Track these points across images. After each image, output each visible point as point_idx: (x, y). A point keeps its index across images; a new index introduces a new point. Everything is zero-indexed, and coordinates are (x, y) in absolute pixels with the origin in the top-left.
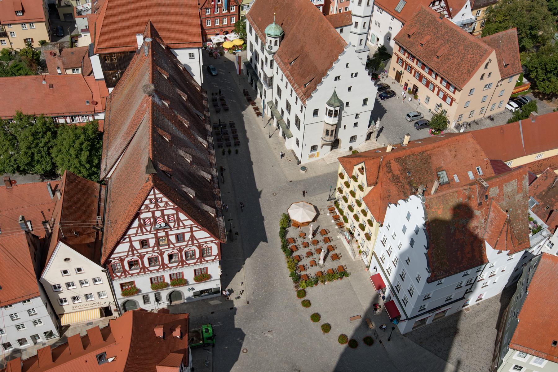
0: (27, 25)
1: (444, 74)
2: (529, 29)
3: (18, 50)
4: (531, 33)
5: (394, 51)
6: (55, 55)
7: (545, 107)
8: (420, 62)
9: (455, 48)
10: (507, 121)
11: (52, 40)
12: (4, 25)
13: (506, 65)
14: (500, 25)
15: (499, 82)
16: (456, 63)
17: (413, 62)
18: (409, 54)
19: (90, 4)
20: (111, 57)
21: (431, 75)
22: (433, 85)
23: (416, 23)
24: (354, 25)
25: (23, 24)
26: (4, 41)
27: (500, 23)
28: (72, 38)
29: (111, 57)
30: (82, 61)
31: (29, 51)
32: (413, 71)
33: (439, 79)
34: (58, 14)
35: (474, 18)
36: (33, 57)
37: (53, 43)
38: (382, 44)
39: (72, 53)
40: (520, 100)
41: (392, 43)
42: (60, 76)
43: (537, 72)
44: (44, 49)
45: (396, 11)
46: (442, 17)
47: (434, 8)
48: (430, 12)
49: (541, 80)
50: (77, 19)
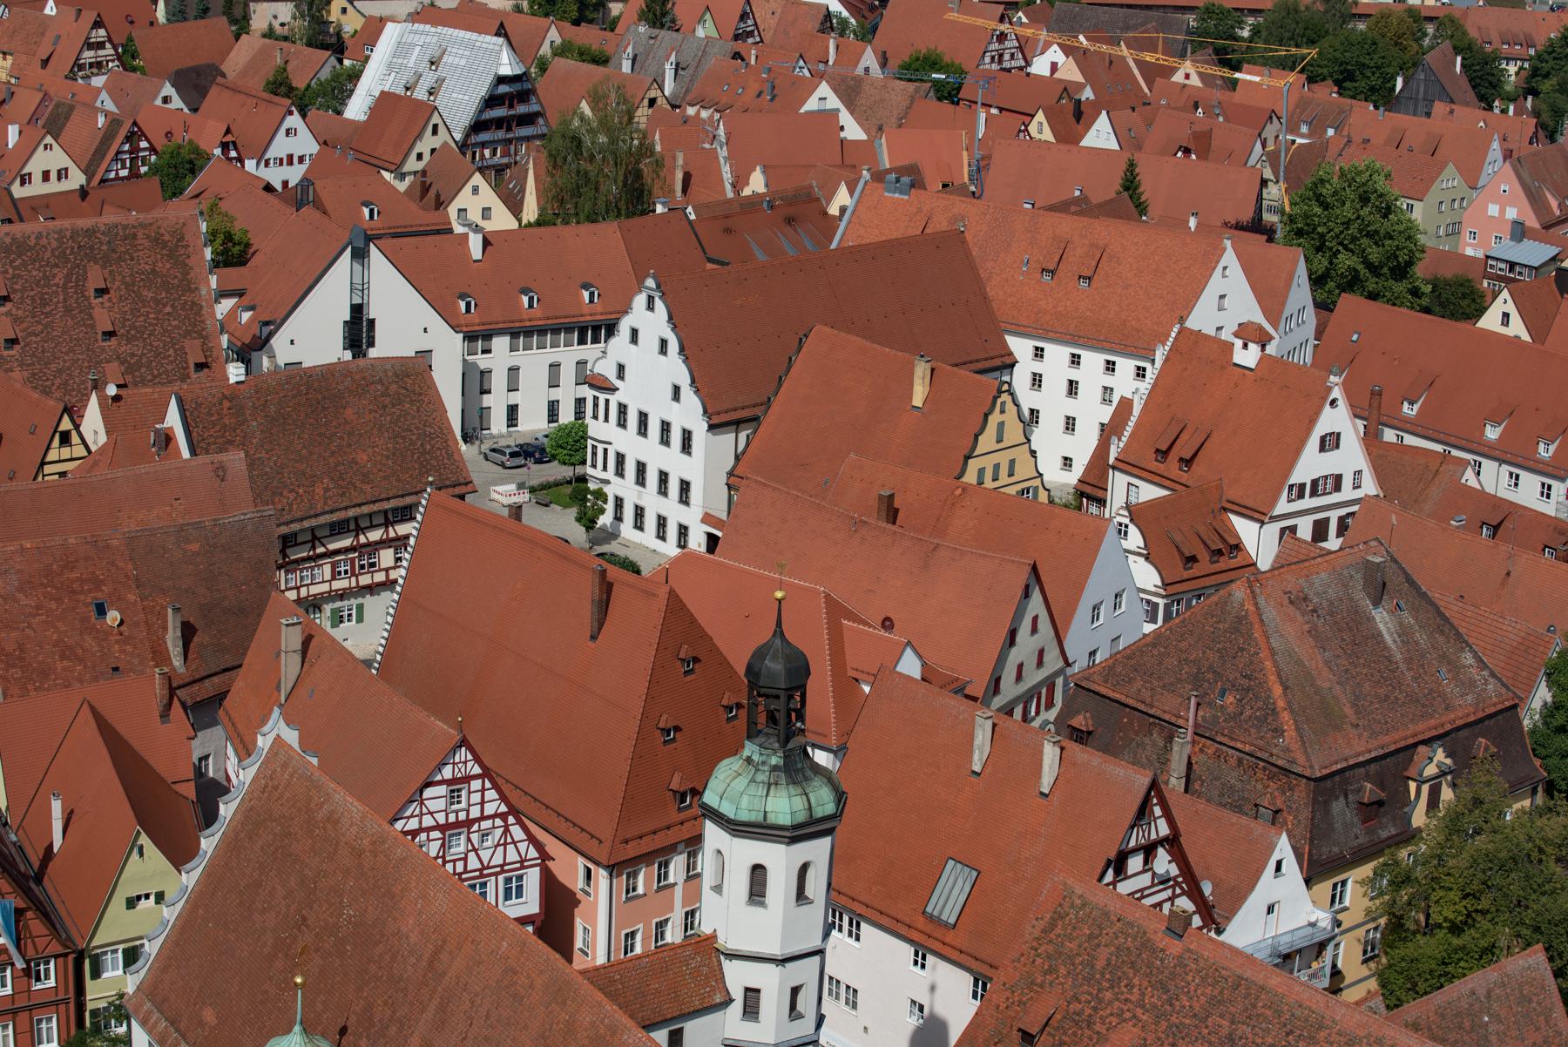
23: (1050, 971)
24: (737, 1007)
27: (1456, 929)
35: (1323, 918)
45: (931, 918)
47: (1124, 888)
48: (1114, 907)
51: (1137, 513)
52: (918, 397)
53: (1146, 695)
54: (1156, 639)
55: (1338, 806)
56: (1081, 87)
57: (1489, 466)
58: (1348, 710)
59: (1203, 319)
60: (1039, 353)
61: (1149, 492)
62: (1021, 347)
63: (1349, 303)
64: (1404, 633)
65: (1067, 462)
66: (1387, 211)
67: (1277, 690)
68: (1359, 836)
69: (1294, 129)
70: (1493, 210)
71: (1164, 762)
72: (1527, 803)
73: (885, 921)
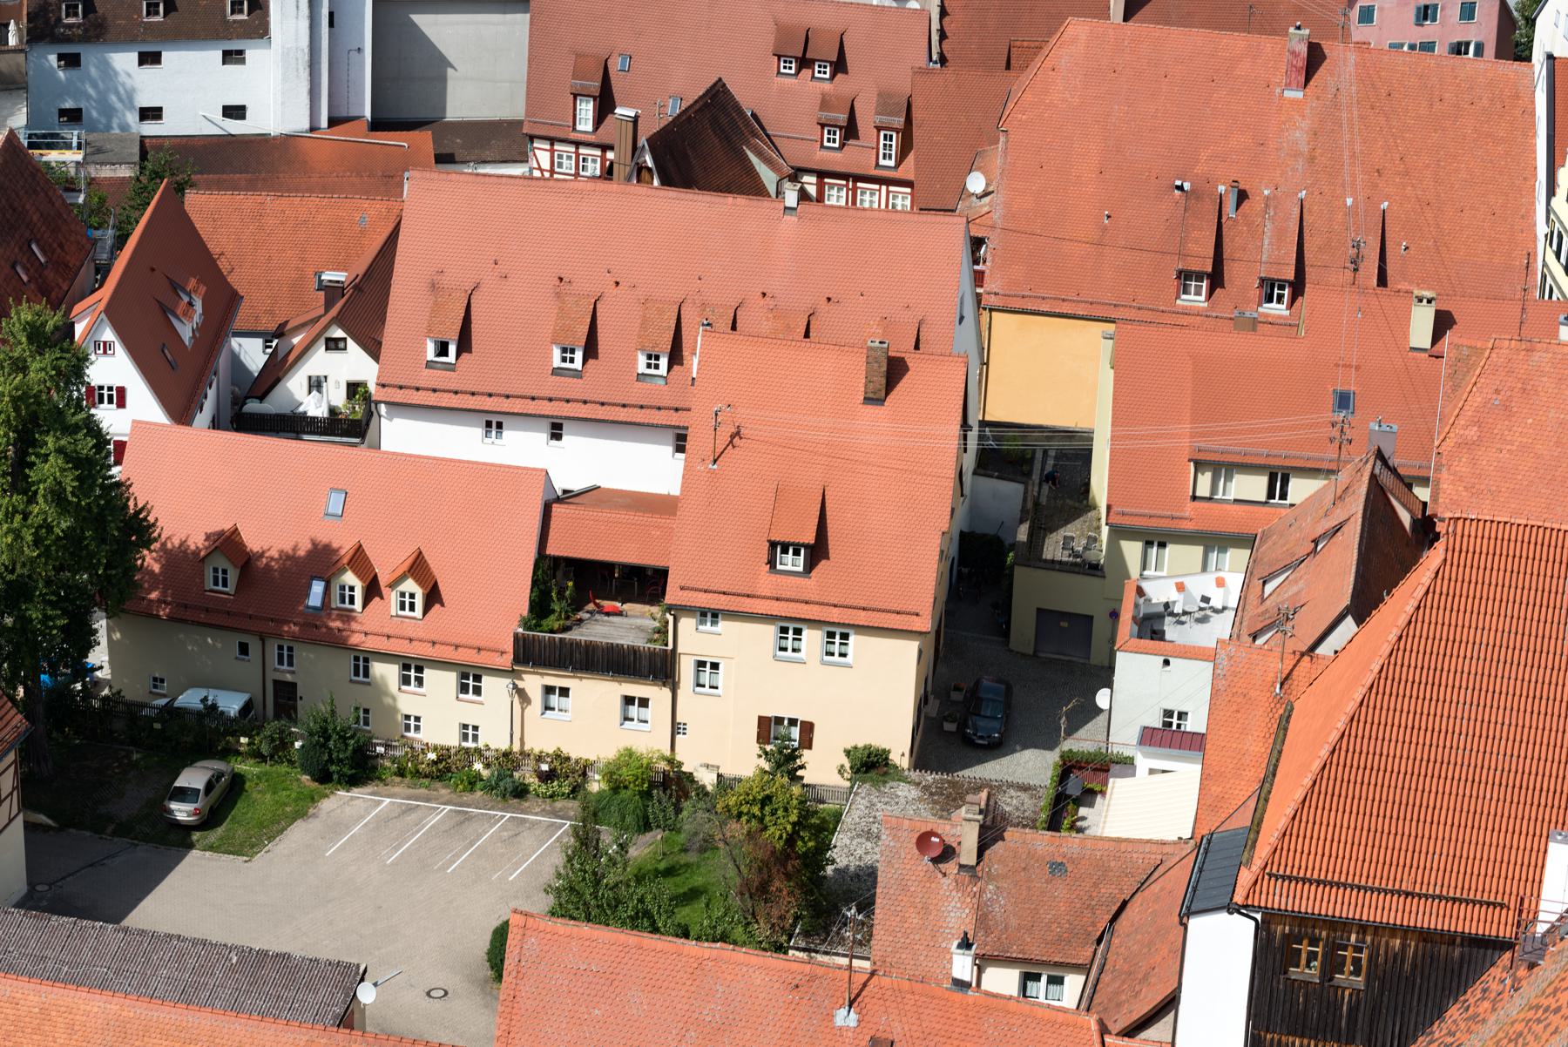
0: (812, 639)
3: (708, 779)
6: (947, 853)
11: (921, 759)
12: (679, 610)
19: (1235, 581)
20: (1333, 948)
25: (790, 628)
26: (644, 703)
28: (1069, 767)
29: (1333, 948)
30: (1109, 938)
31: (780, 799)
34: (1004, 607)
36: (791, 841)
37: (930, 778)
39: (1057, 868)
42: (958, 996)
44: (861, 803)
50: (1123, 661)
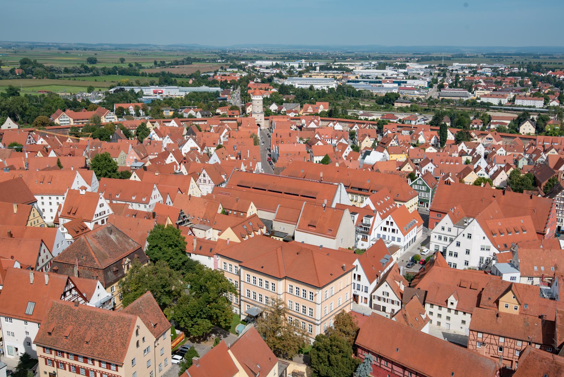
1: (100, 356)
2: (162, 288)
4: (165, 291)
5: (38, 355)
7: (204, 349)
8: (71, 354)
9: (101, 328)
10: (177, 375)
13: (155, 325)
14: (136, 293)
15: (155, 342)
16: (107, 341)
17: (63, 357)
18: (56, 351)
21: (87, 363)
22: (93, 371)
27: (135, 291)
32: (67, 366)
33: (97, 363)
38: (23, 351)
40: (181, 351)
41: (34, 347)
43: (184, 321)
46: (77, 304)
47: (66, 299)
48: (63, 303)
49: (191, 326)
51: (65, 225)
52: (15, 211)
53: (67, 260)
54: (68, 249)
55: (109, 273)
56: (47, 145)
57: (134, 204)
58: (108, 255)
59: (75, 186)
60: (42, 198)
61: (67, 221)
62: (38, 198)
63: (102, 179)
64: (117, 238)
65: (52, 217)
66: (110, 161)
67: (93, 254)
68: (114, 277)
69: (91, 148)
70: (131, 158)
71: (73, 272)
72: (146, 264)
73: (17, 317)
